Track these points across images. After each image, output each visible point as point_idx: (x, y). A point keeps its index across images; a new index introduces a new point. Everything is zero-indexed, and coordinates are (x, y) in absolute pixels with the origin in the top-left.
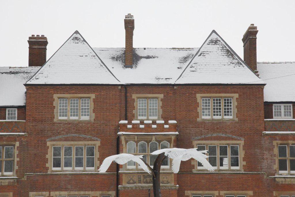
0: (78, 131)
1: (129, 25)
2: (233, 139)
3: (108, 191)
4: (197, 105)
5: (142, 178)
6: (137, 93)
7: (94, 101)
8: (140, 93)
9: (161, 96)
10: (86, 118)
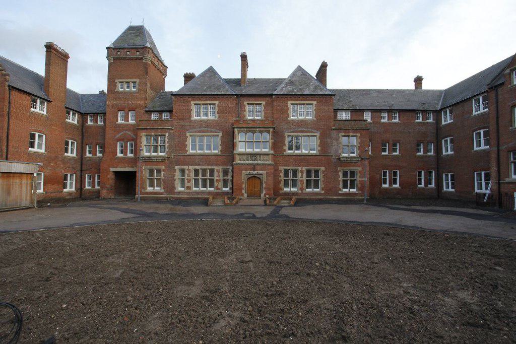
0: (207, 126)
1: (244, 57)
2: (312, 132)
3: (227, 166)
4: (288, 109)
5: (249, 157)
6: (247, 101)
7: (219, 106)
8: (249, 101)
9: (264, 103)
10: (213, 118)
